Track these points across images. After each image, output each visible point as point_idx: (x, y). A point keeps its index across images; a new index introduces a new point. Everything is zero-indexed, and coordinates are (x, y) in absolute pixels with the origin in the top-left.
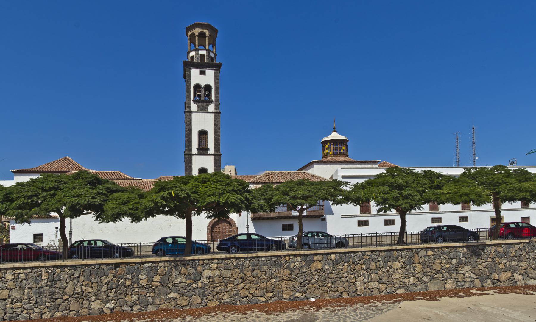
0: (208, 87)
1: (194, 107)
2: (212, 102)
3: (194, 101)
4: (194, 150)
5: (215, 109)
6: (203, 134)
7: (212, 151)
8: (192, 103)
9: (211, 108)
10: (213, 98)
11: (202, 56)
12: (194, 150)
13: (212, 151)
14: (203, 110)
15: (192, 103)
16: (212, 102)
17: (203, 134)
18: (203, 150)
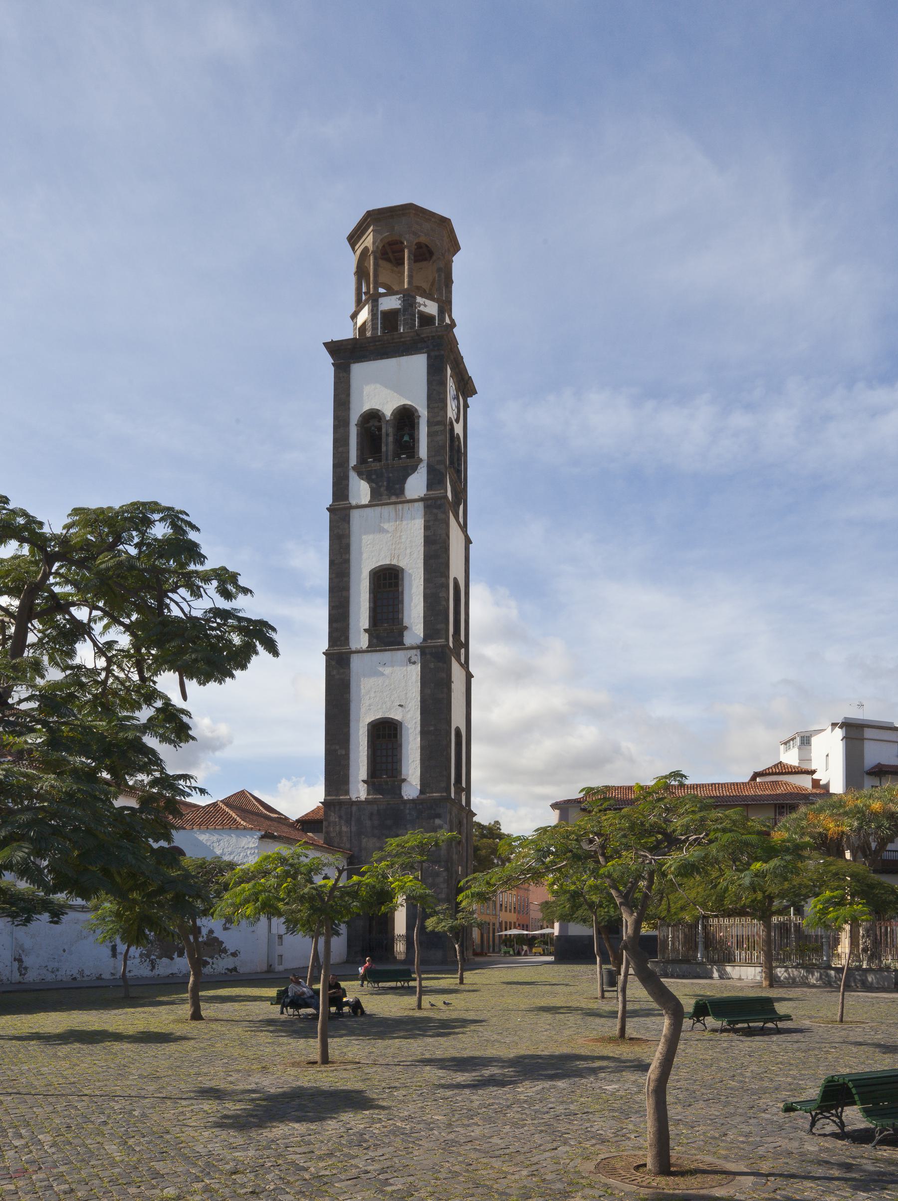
1: (360, 490)
4: (360, 639)
5: (430, 486)
6: (387, 581)
8: (353, 476)
9: (416, 485)
12: (360, 639)
15: (353, 476)
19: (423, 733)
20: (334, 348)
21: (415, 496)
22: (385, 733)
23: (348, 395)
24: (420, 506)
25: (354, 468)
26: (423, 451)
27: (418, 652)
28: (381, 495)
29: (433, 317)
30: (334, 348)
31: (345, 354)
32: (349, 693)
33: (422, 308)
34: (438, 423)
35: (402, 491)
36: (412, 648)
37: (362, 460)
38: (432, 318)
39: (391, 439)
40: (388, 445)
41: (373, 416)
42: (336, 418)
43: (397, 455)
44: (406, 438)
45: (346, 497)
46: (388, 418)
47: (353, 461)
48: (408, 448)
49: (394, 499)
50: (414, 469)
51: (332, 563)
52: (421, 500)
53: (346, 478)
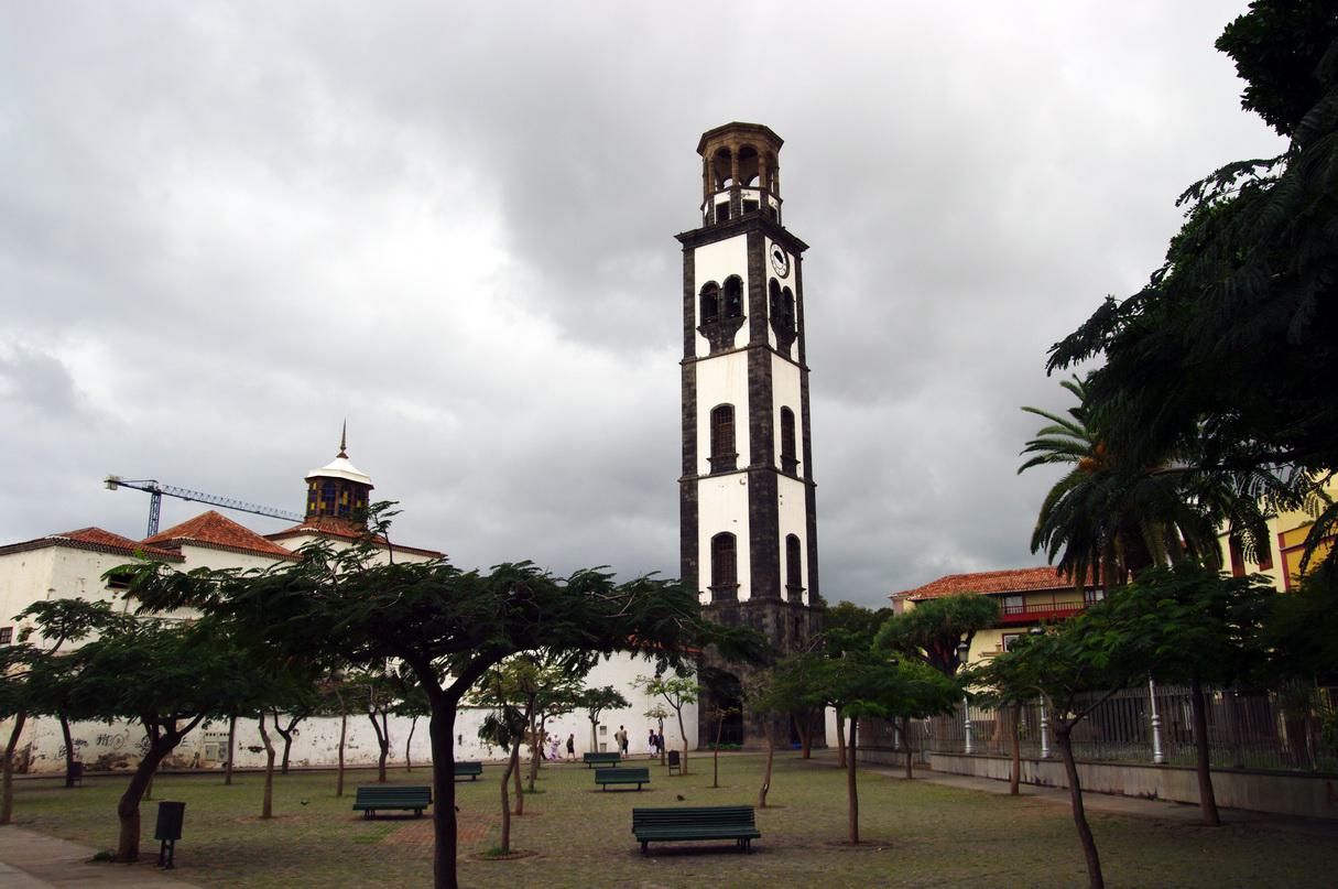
0: (734, 283)
1: (702, 345)
2: (745, 318)
3: (699, 329)
4: (704, 467)
6: (723, 415)
7: (744, 460)
9: (743, 337)
10: (746, 312)
11: (723, 207)
12: (704, 467)
13: (744, 460)
14: (722, 345)
15: (698, 334)
16: (745, 318)
17: (723, 415)
18: (723, 462)
19: (752, 543)
20: (682, 238)
21: (741, 347)
22: (724, 543)
23: (694, 272)
24: (745, 354)
25: (699, 329)
26: (746, 312)
27: (746, 474)
28: (718, 348)
29: (756, 202)
30: (682, 238)
31: (691, 241)
32: (697, 512)
33: (746, 198)
34: (757, 286)
35: (733, 342)
36: (742, 471)
37: (703, 321)
38: (755, 202)
39: (723, 303)
40: (722, 309)
41: (710, 287)
42: (685, 291)
43: (728, 316)
44: (736, 301)
45: (694, 352)
46: (721, 286)
47: (698, 323)
48: (739, 307)
49: (727, 350)
50: (741, 325)
51: (684, 406)
52: (745, 349)
53: (694, 337)
